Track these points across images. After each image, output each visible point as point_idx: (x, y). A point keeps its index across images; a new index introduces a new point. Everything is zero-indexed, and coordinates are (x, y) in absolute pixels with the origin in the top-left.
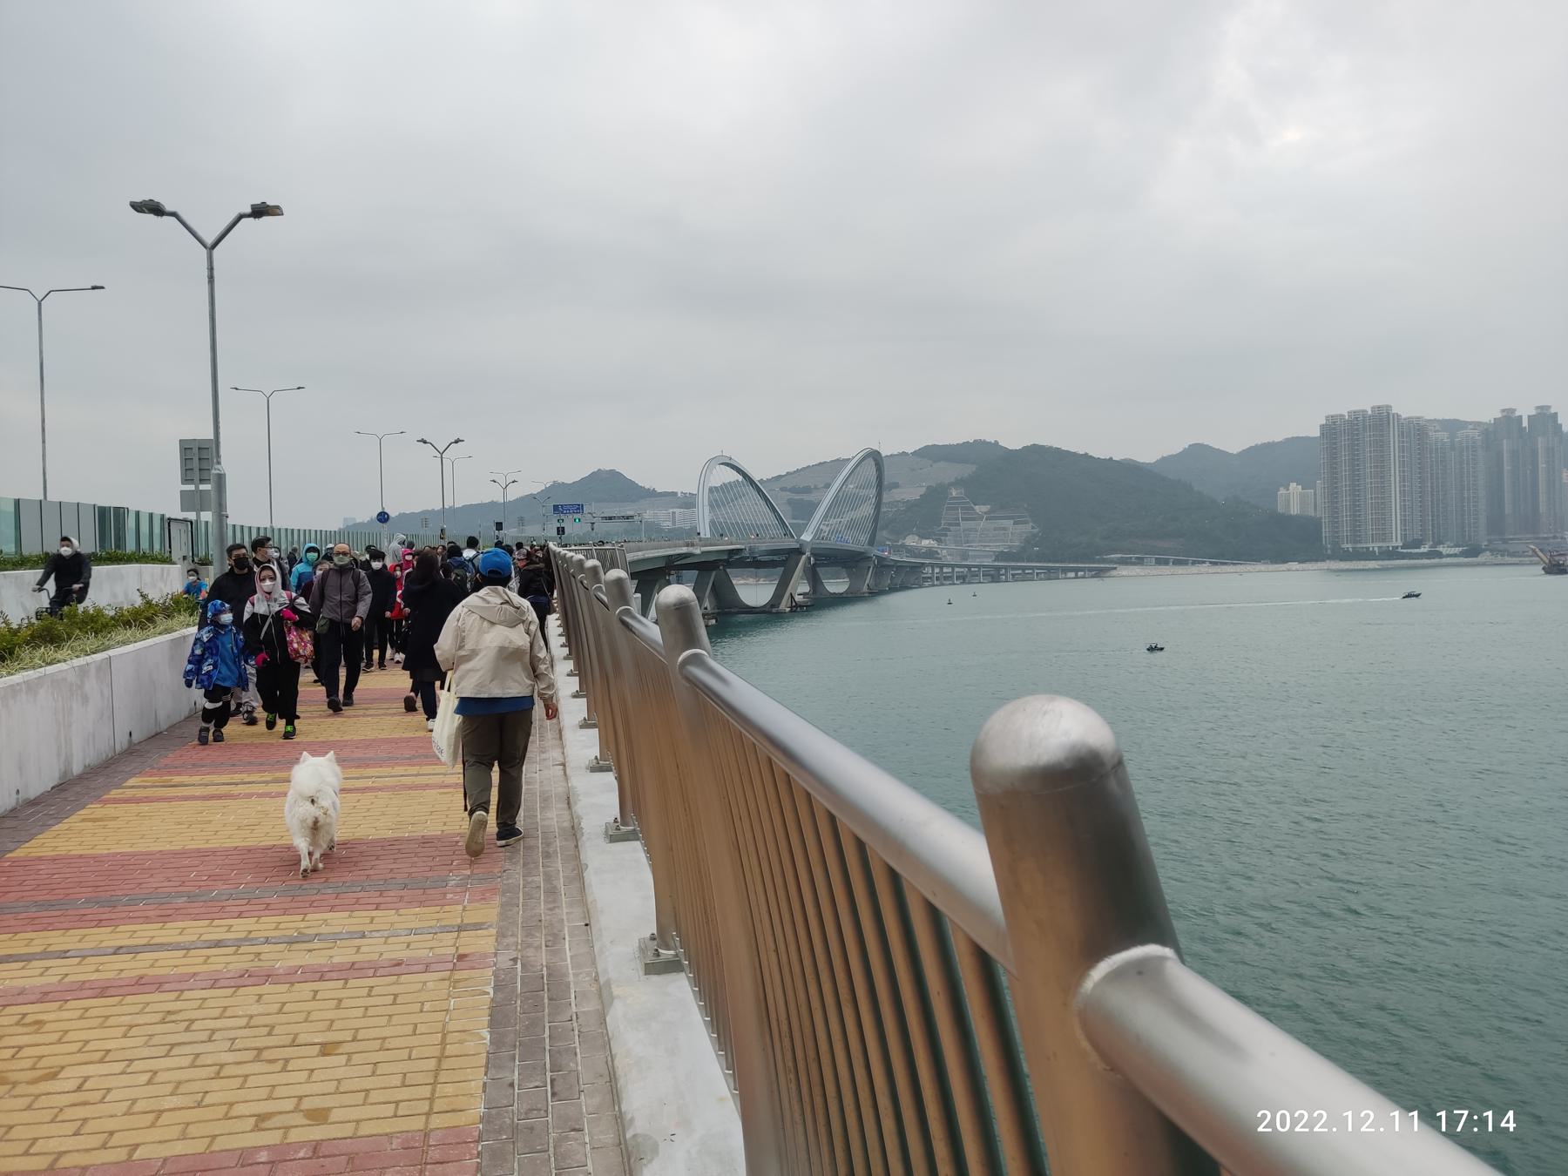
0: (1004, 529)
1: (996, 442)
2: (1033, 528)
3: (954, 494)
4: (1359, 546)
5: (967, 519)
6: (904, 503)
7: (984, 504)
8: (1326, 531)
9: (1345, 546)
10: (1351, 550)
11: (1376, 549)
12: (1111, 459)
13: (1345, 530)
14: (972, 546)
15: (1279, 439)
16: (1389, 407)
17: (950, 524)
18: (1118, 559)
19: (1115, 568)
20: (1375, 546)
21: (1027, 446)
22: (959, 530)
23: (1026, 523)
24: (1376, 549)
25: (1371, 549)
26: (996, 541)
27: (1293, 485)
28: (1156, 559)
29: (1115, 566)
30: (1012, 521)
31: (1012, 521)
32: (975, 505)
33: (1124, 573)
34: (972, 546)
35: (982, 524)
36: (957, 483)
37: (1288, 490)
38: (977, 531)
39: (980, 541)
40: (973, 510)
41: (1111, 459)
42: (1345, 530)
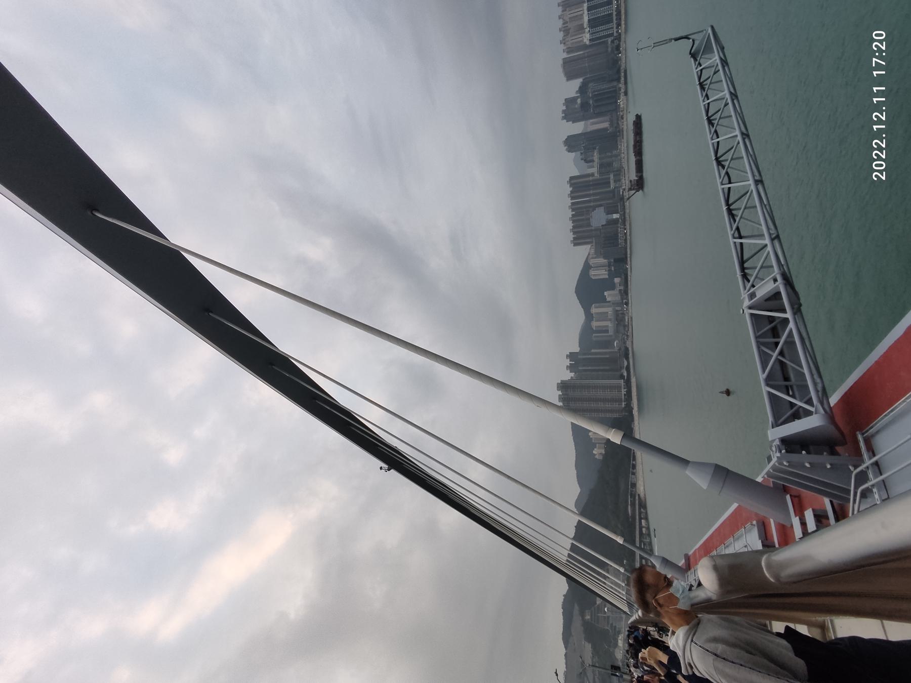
1: (564, 596)
3: (588, 617)
8: (616, 415)
9: (623, 406)
11: (625, 390)
12: (575, 527)
13: (616, 406)
15: (575, 472)
16: (558, 384)
17: (608, 623)
18: (631, 507)
19: (639, 495)
20: (624, 391)
24: (625, 390)
25: (625, 393)
27: (594, 452)
28: (631, 487)
29: (637, 498)
32: (596, 604)
33: (642, 488)
36: (582, 614)
37: (596, 454)
40: (599, 604)
41: (575, 527)
42: (616, 406)
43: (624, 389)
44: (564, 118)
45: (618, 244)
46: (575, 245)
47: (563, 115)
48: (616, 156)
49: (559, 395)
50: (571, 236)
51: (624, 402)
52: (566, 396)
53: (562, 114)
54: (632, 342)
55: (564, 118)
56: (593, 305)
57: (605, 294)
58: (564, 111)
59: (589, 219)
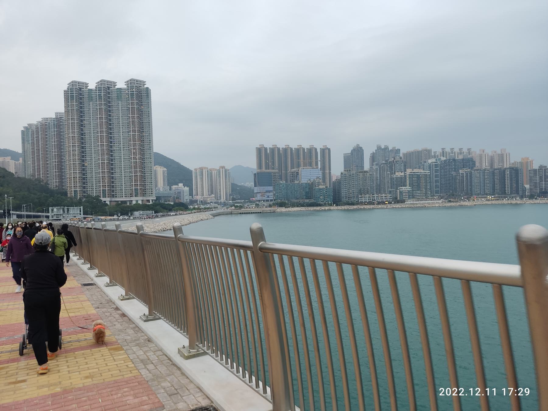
4: (114, 199)
9: (103, 199)
10: (108, 203)
16: (144, 83)
43: (142, 200)
44: (379, 148)
45: (361, 194)
46: (260, 151)
47: (383, 147)
48: (426, 193)
49: (114, 84)
50: (268, 145)
51: (110, 201)
52: (114, 95)
53: (385, 146)
54: (231, 213)
55: (379, 148)
56: (166, 169)
57: (179, 184)
58: (386, 148)
59: (305, 165)
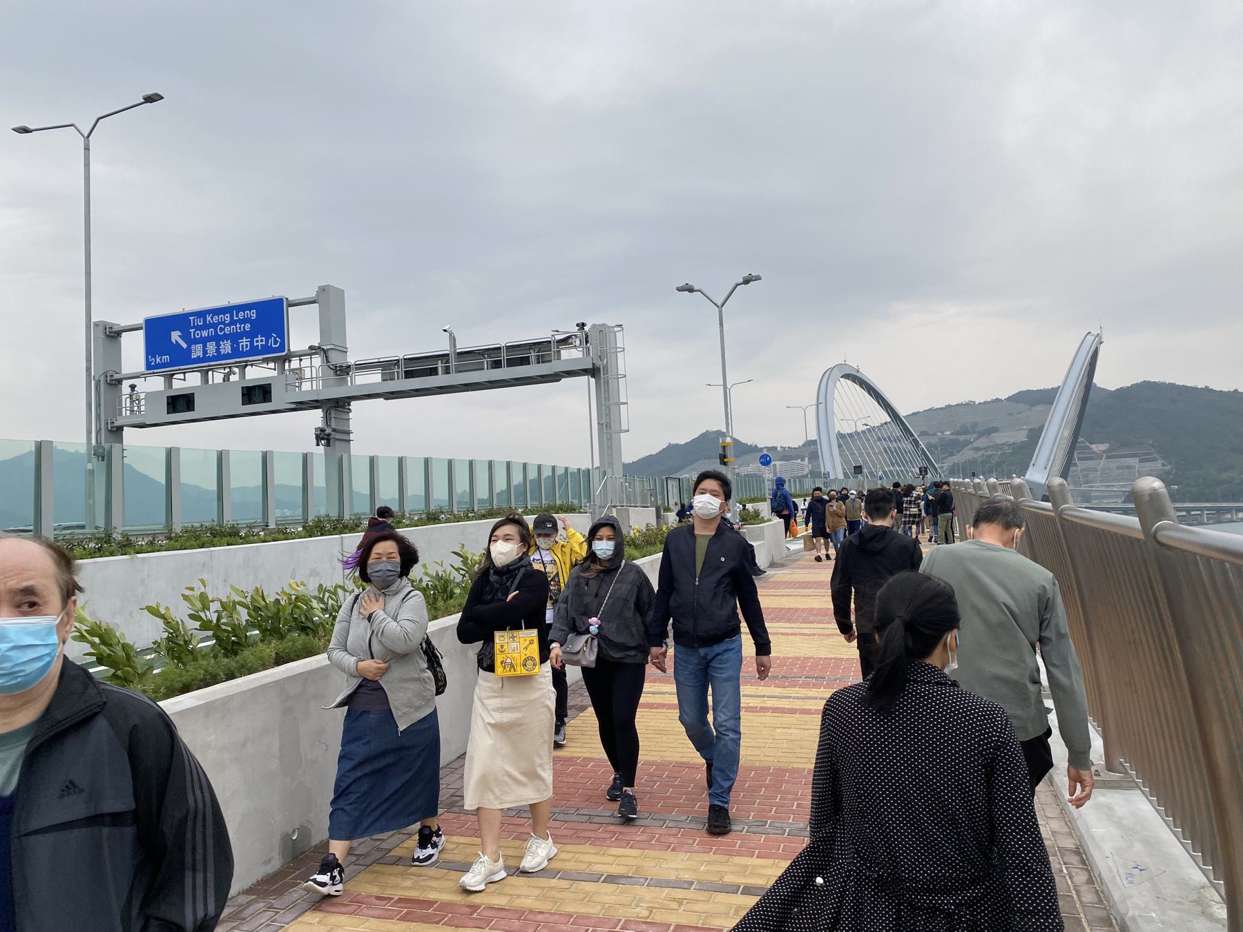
0: (1129, 467)
2: (1163, 465)
5: (1087, 459)
6: (1009, 445)
7: (1102, 442)
14: (1093, 486)
21: (1150, 382)
22: (1077, 471)
23: (1154, 460)
26: (1119, 480)
30: (1138, 459)
31: (1138, 459)
34: (1093, 486)
35: (1102, 463)
38: (1097, 471)
39: (1101, 482)
40: (1090, 449)
